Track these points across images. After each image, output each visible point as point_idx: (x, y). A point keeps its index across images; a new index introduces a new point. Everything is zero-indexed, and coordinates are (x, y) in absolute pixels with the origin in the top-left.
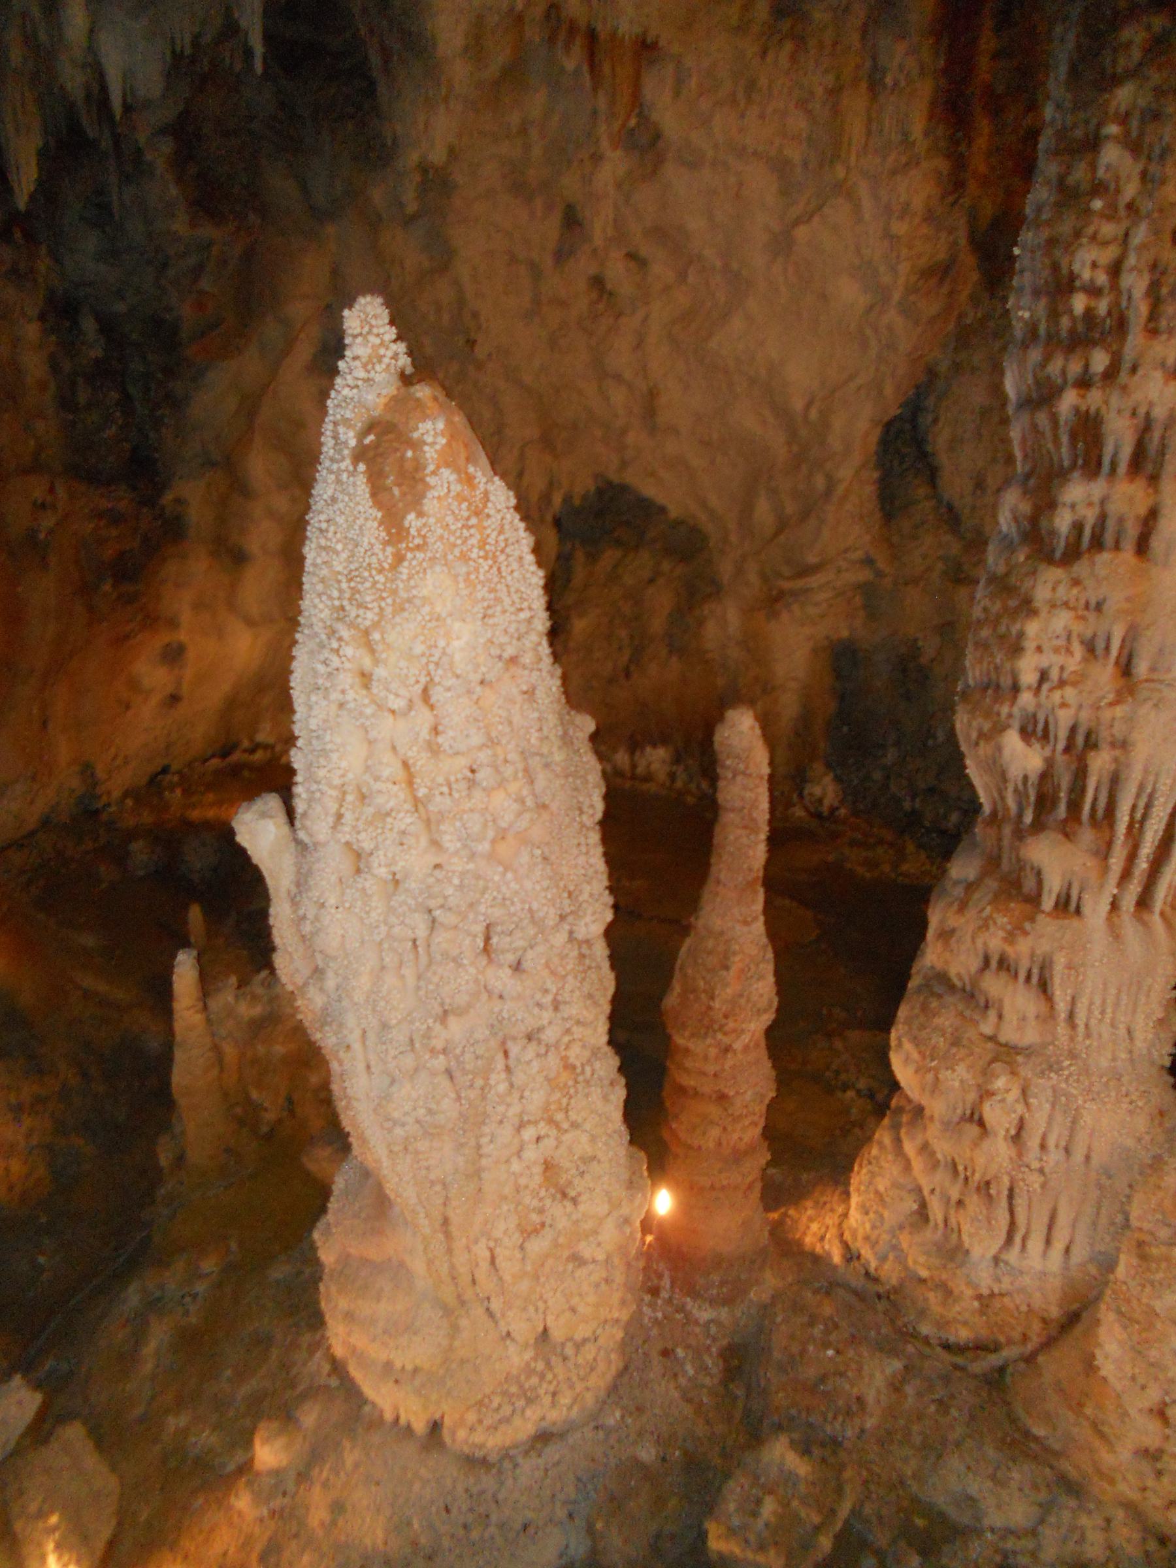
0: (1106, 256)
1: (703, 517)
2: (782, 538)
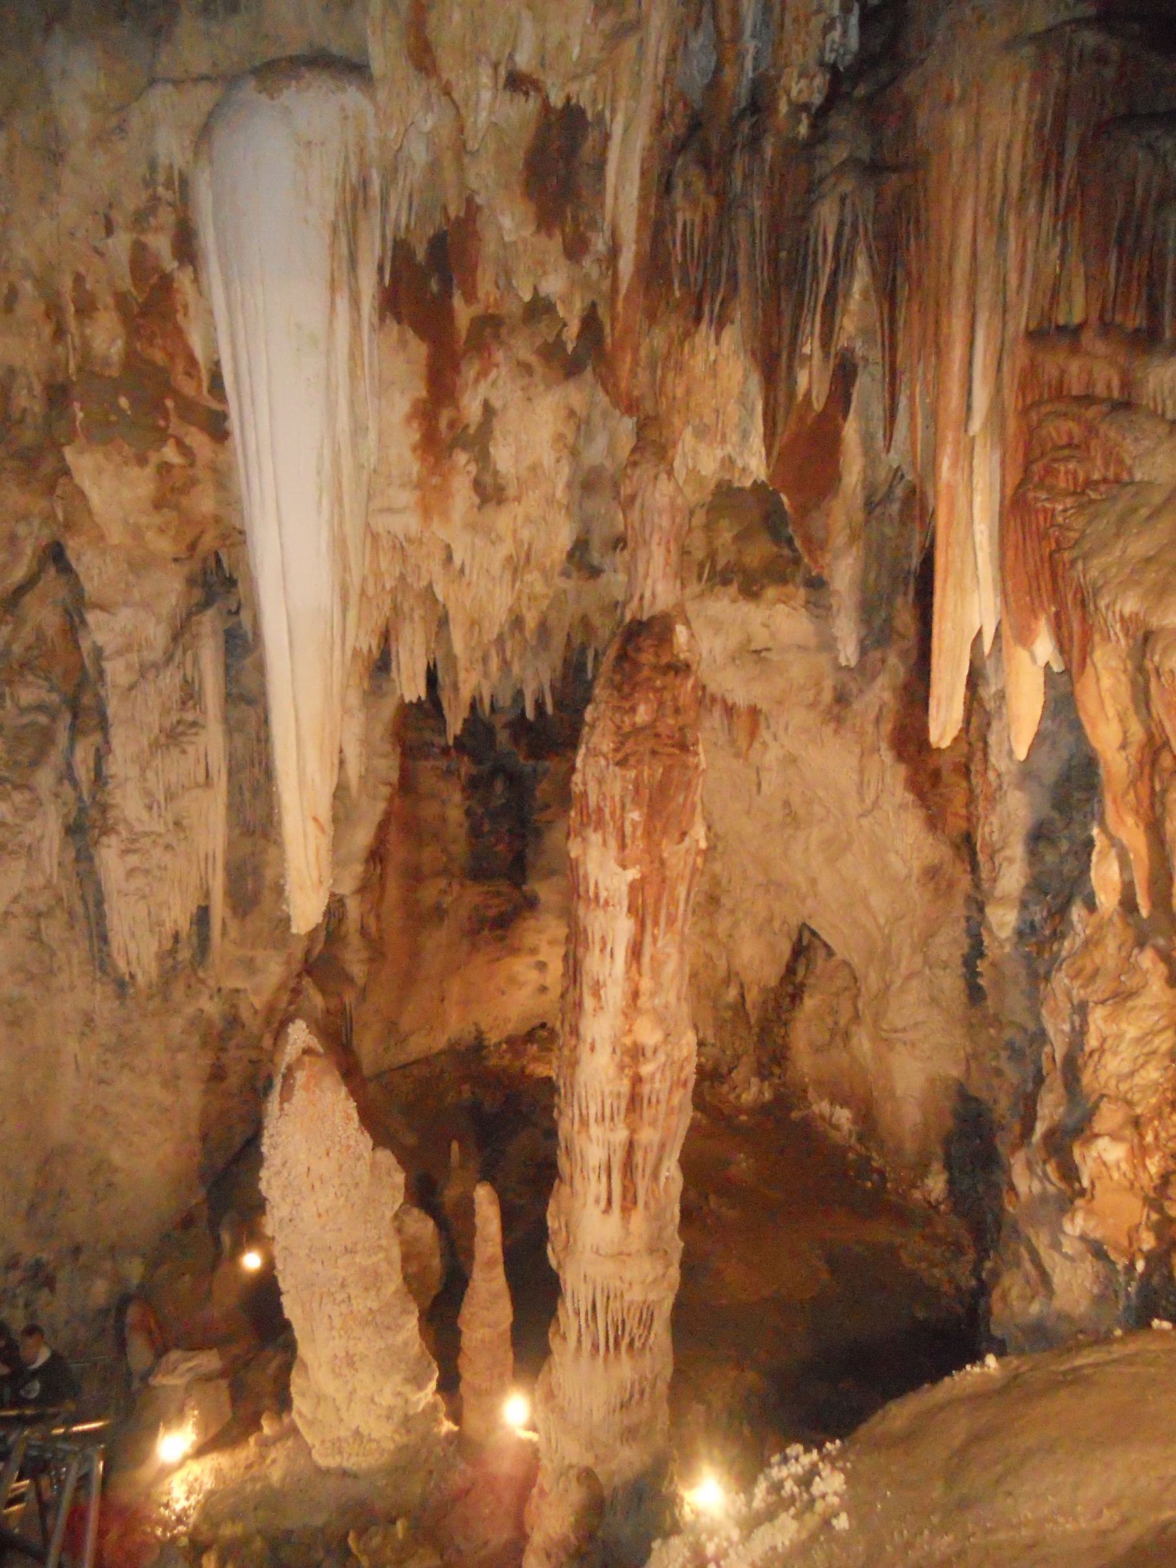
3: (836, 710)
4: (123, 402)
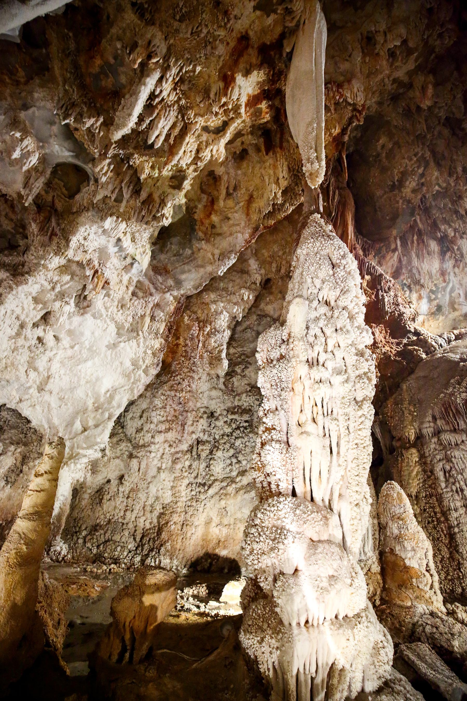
1: (46, 426)
2: (86, 433)
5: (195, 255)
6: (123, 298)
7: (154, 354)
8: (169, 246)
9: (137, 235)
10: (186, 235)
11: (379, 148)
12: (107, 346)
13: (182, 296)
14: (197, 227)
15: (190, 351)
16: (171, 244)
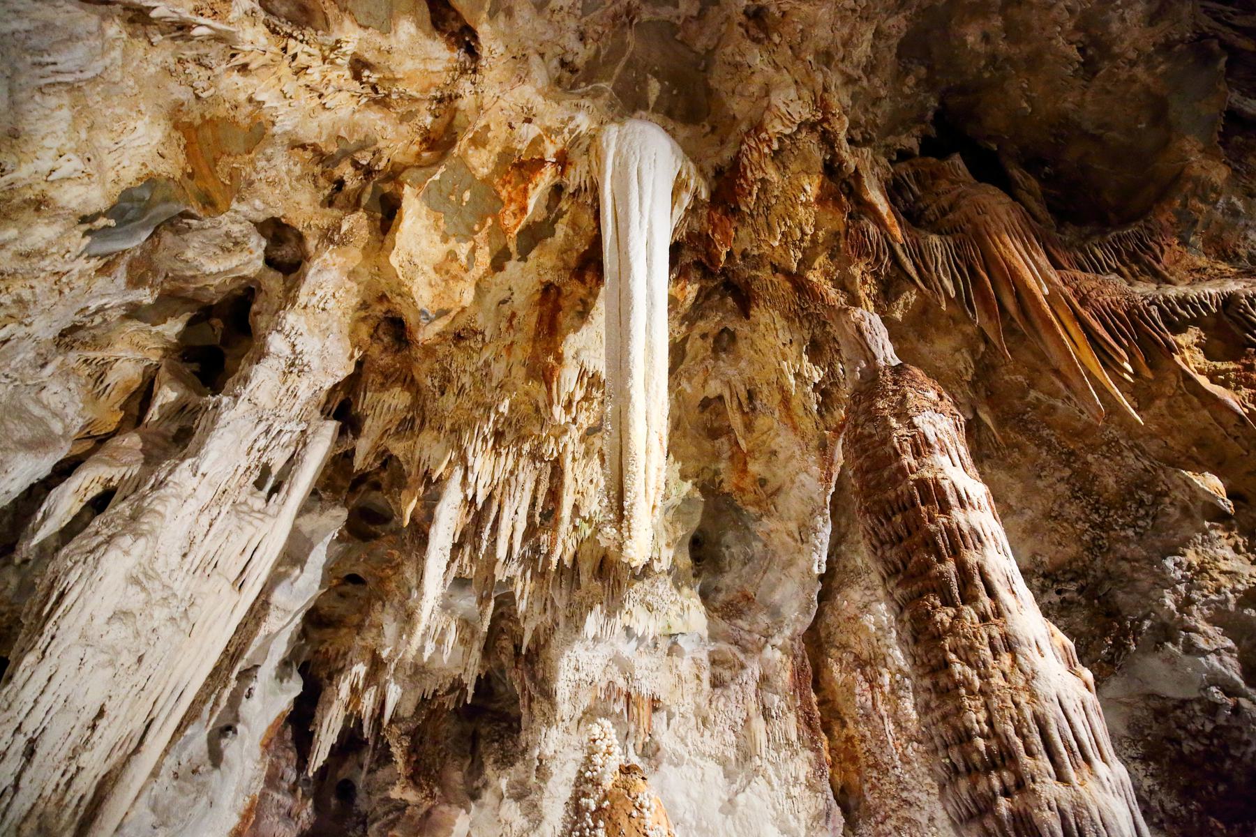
0: (982, 716)
3: (718, 691)
4: (467, 196)
5: (771, 547)
6: (698, 707)
7: (810, 787)
8: (727, 553)
9: (648, 598)
10: (736, 523)
11: (981, 48)
12: (721, 810)
13: (793, 639)
14: (739, 503)
15: (878, 751)
16: (728, 547)
